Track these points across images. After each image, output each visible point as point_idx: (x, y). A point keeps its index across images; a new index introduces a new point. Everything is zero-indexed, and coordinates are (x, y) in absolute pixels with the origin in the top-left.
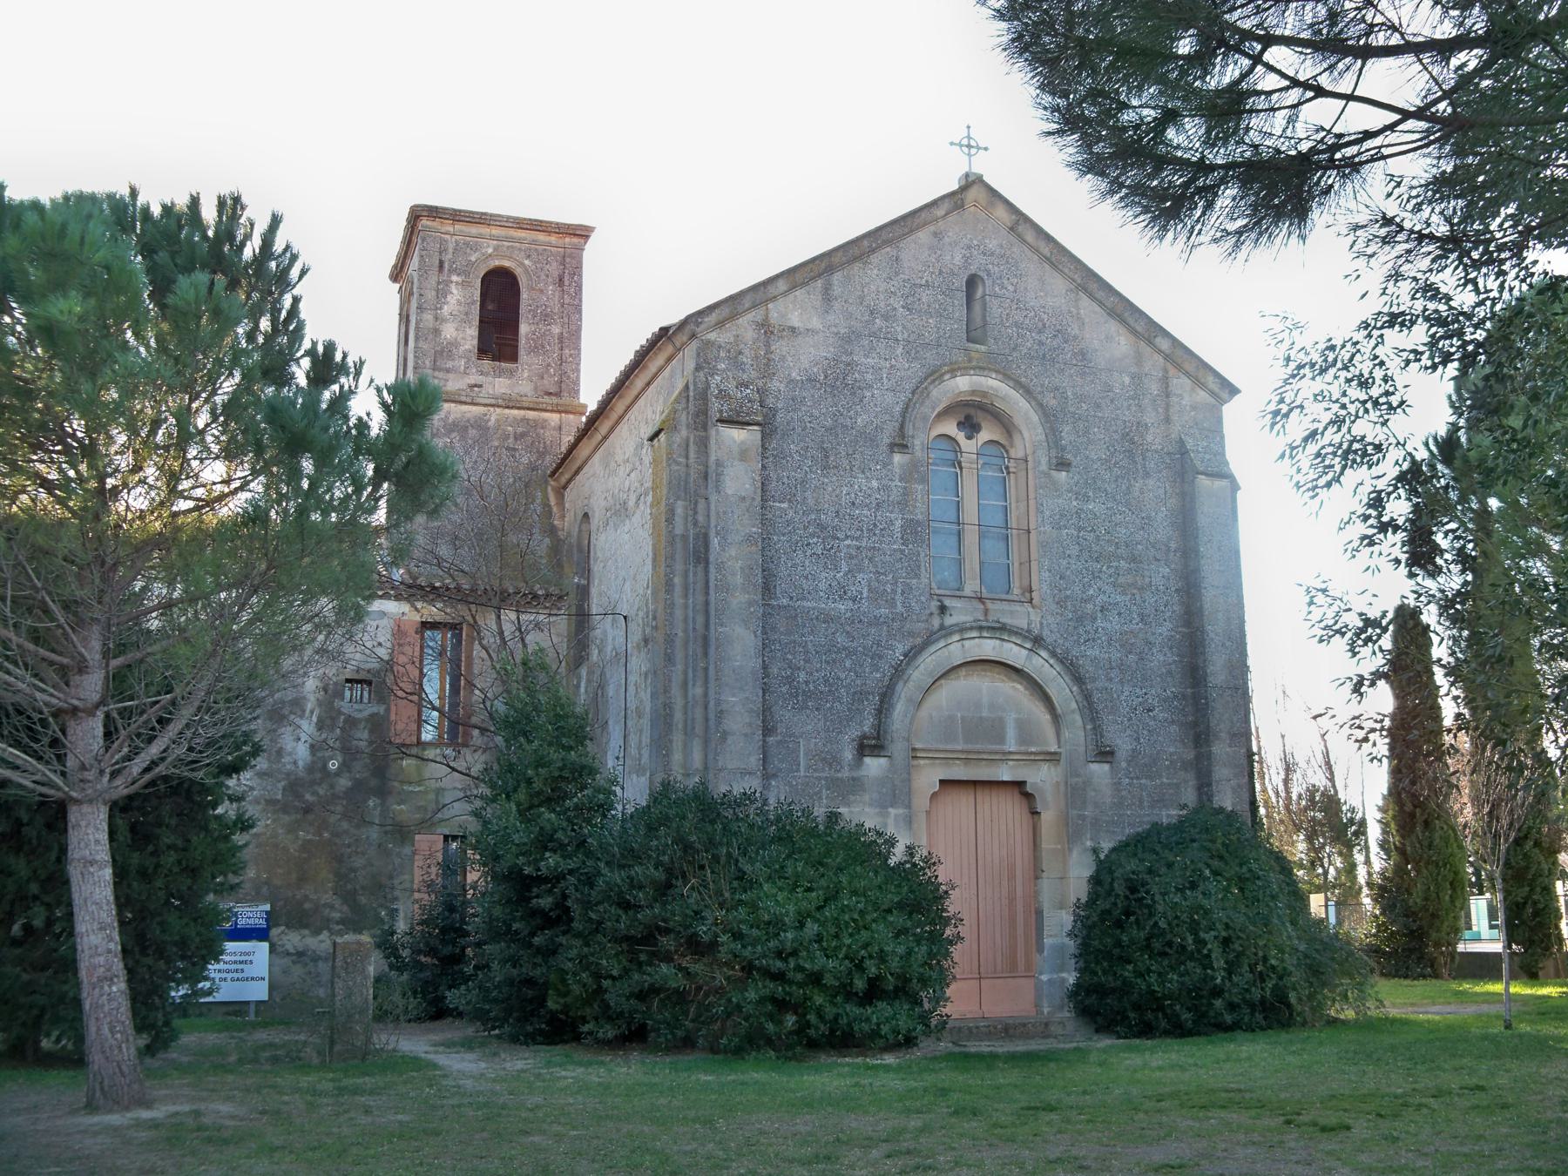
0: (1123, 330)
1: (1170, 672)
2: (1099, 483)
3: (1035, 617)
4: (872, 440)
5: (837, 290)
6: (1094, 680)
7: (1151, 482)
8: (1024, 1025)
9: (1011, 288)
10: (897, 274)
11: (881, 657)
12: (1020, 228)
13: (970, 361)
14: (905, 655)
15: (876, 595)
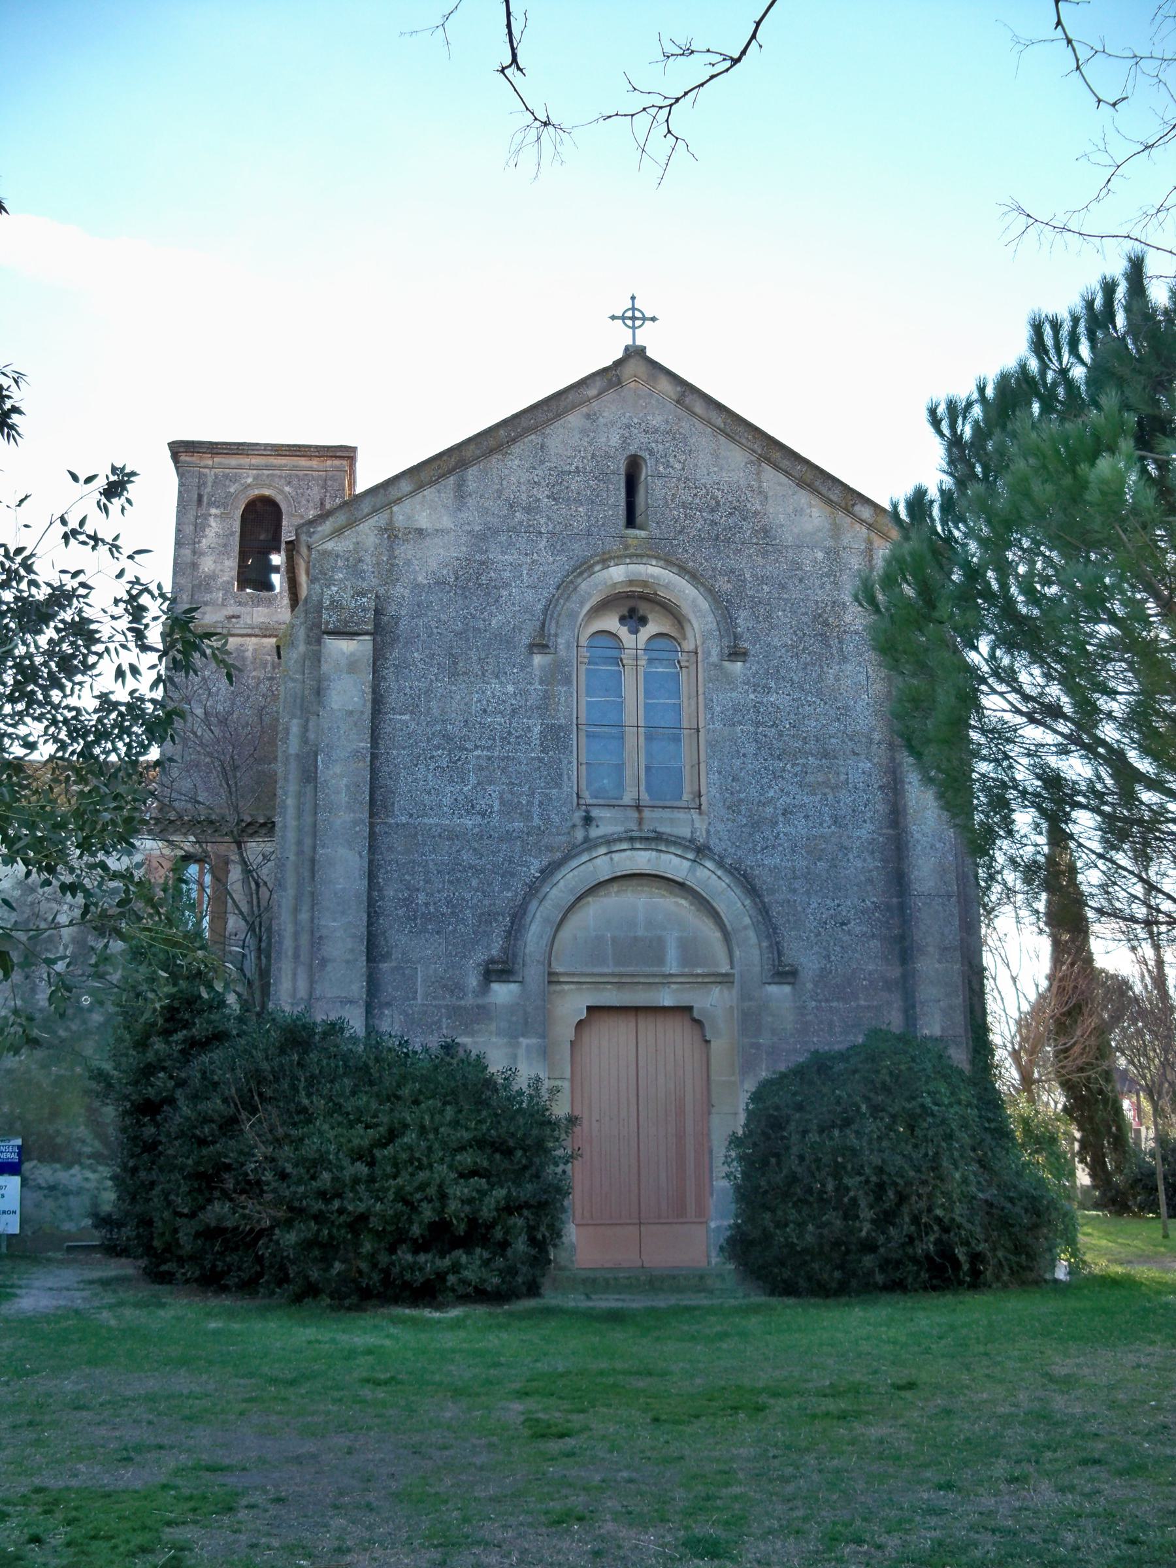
0: (815, 501)
1: (870, 881)
2: (783, 672)
3: (701, 824)
4: (506, 640)
5: (471, 486)
6: (772, 892)
7: (849, 667)
8: (674, 1277)
9: (678, 466)
10: (542, 462)
11: (513, 875)
12: (687, 400)
13: (626, 548)
14: (542, 872)
15: (509, 807)
